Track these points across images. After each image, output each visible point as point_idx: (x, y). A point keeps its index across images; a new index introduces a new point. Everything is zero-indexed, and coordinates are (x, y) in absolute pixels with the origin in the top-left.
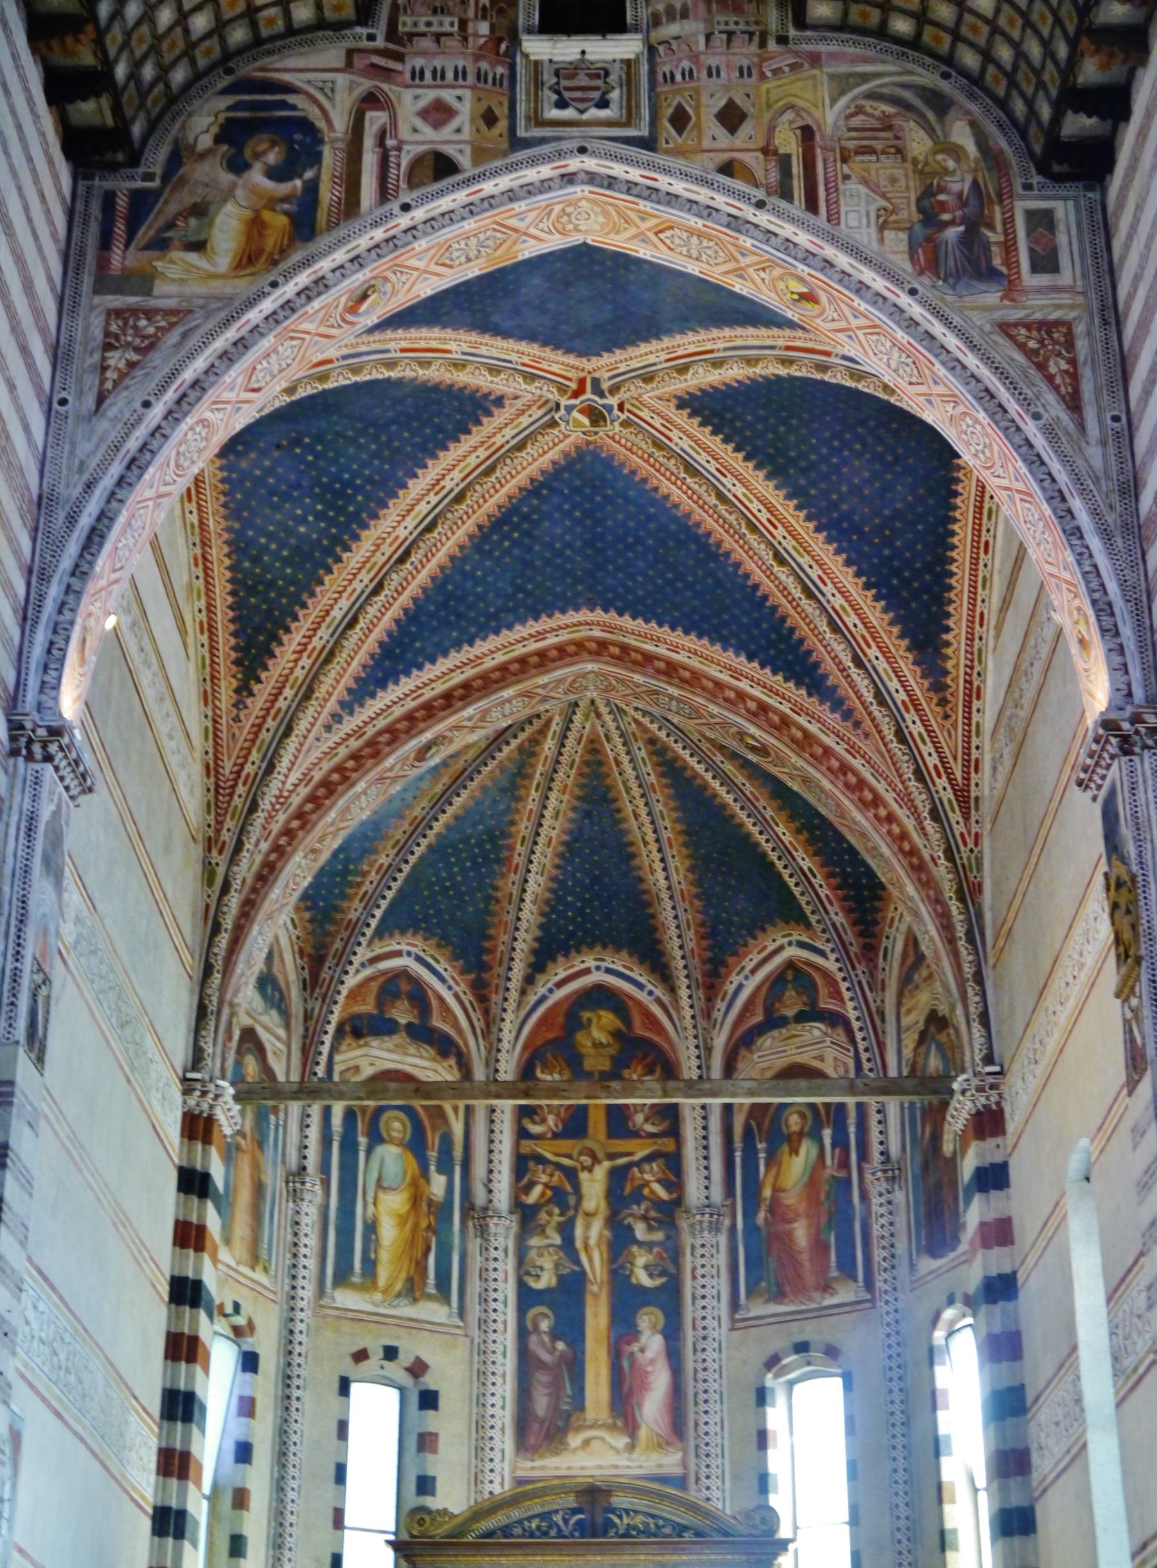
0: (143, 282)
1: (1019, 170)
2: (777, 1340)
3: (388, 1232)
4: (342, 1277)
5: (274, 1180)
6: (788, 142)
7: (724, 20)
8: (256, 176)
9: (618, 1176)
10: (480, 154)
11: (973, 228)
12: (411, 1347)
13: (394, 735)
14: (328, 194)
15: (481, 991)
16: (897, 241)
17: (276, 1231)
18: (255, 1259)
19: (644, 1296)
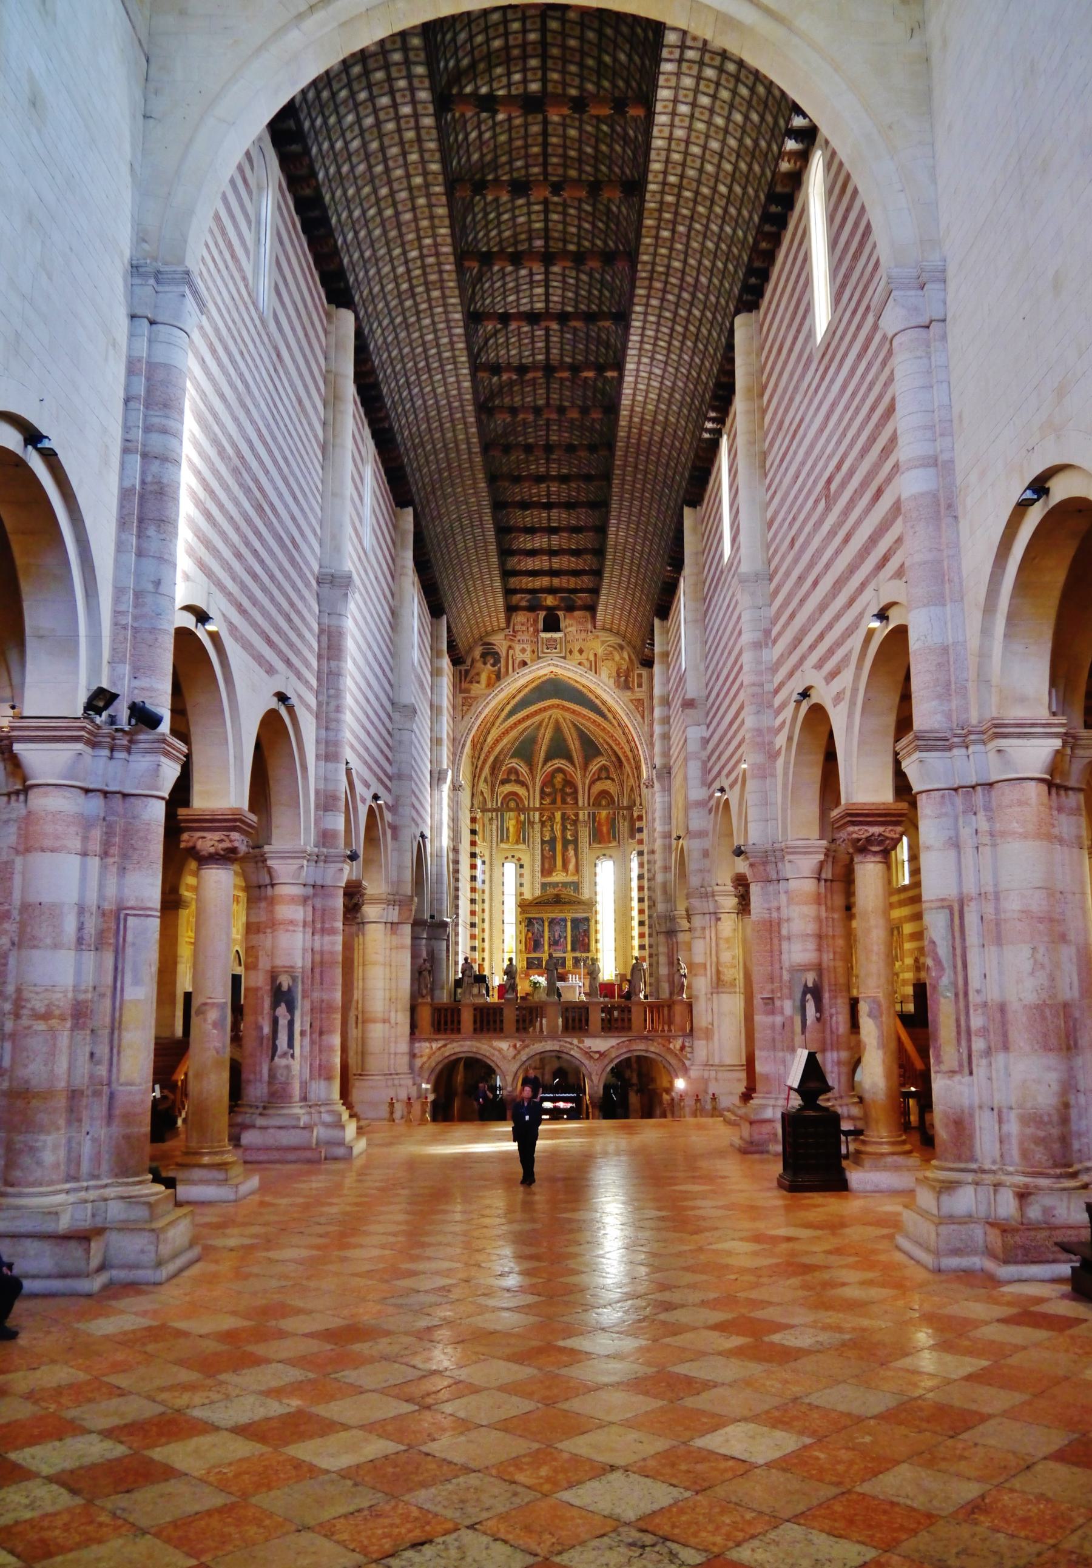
0: (468, 691)
1: (636, 663)
2: (599, 853)
3: (511, 829)
4: (502, 841)
5: (487, 821)
6: (592, 658)
7: (580, 627)
8: (489, 666)
9: (563, 815)
10: (532, 661)
11: (627, 677)
12: (517, 855)
13: (512, 728)
14: (503, 670)
15: (531, 770)
16: (612, 681)
17: (487, 833)
18: (484, 840)
19: (569, 842)
